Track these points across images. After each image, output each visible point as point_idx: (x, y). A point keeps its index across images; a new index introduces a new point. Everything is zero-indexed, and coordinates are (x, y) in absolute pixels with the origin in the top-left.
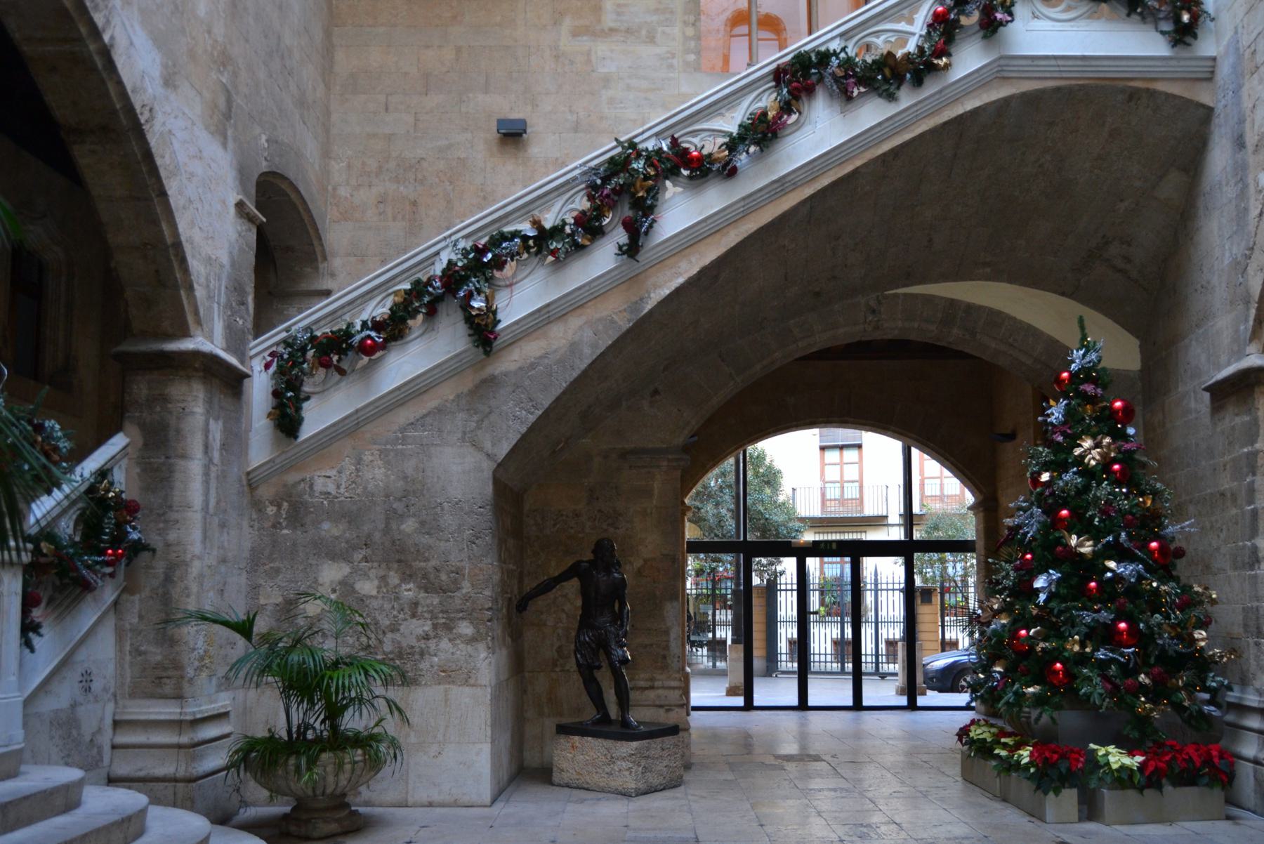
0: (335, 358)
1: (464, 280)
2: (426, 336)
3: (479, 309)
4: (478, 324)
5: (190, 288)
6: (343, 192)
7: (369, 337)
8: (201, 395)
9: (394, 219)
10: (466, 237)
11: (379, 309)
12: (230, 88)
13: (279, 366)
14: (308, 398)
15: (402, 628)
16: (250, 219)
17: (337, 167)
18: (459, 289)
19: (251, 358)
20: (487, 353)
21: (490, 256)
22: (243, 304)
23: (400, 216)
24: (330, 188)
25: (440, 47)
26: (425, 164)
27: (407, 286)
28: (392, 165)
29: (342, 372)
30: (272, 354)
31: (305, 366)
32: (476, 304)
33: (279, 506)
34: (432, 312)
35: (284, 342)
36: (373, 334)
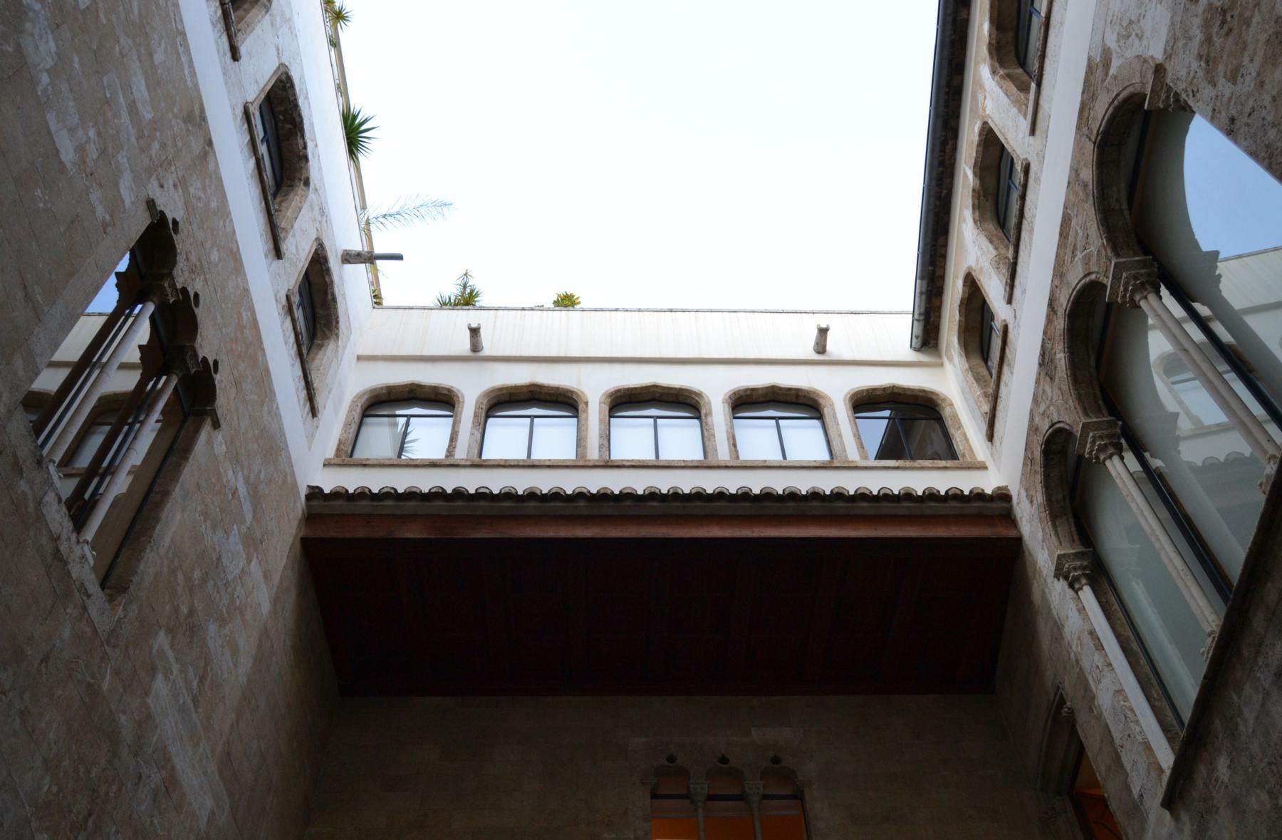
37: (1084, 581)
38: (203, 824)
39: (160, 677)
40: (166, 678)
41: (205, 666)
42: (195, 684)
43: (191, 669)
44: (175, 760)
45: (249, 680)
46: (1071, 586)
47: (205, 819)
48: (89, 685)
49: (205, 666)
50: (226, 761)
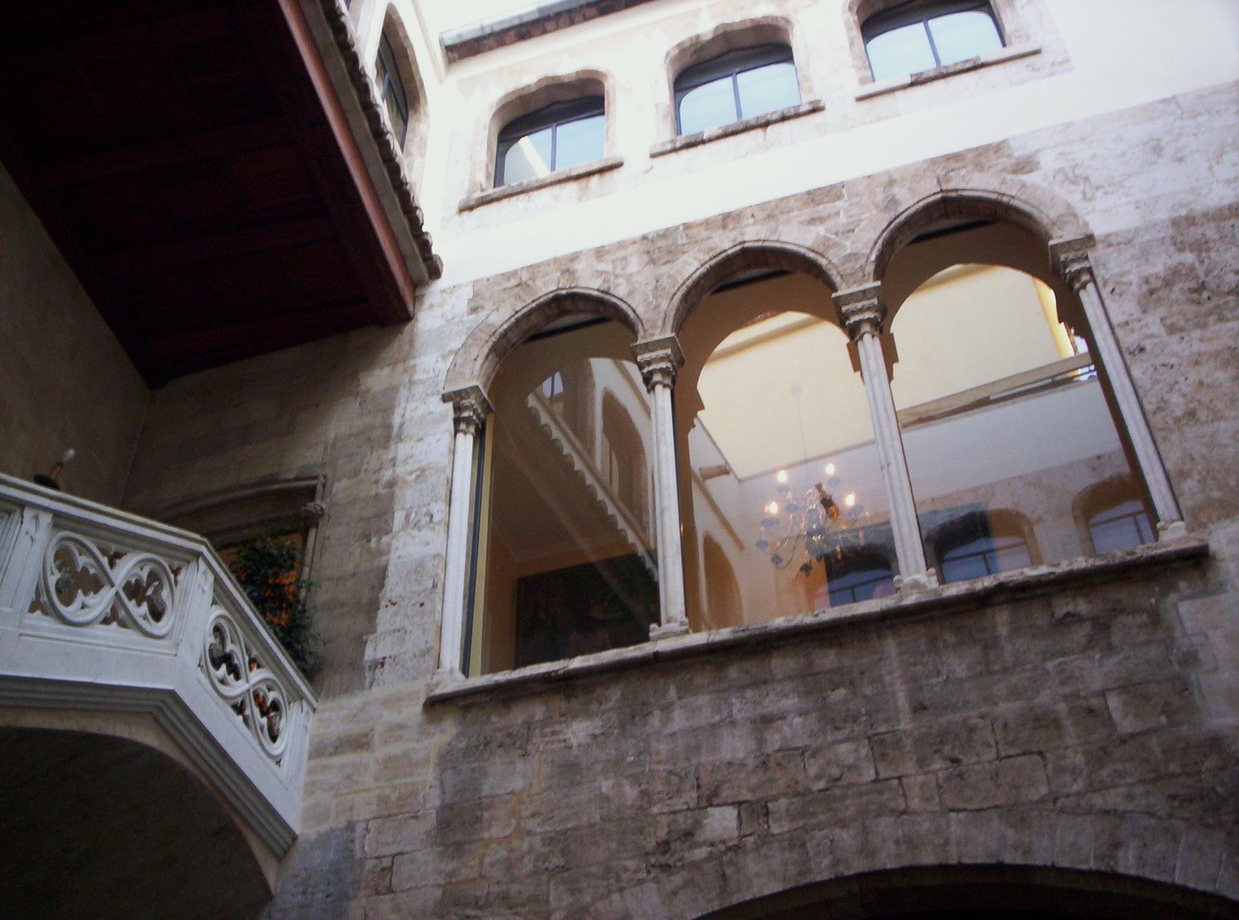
37: (472, 429)
46: (457, 421)
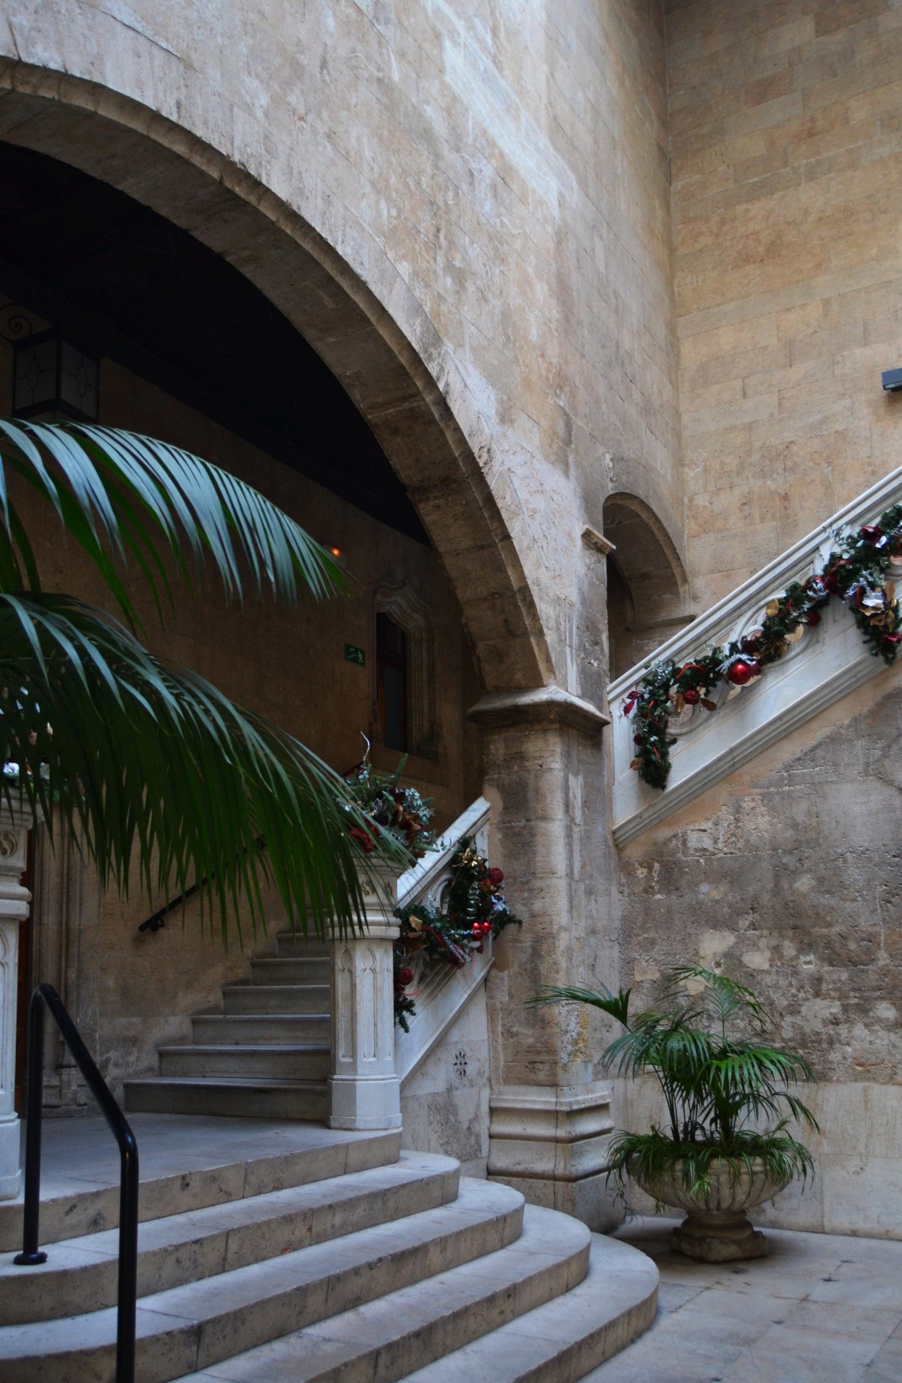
0: (702, 691)
1: (854, 575)
2: (810, 651)
3: (874, 608)
4: (876, 627)
5: (541, 634)
6: (701, 501)
7: (740, 661)
8: (558, 749)
9: (763, 520)
10: (851, 522)
11: (750, 627)
12: (568, 410)
13: (640, 708)
14: (674, 741)
15: (803, 1010)
16: (598, 548)
17: (692, 474)
18: (847, 587)
19: (609, 703)
20: (890, 661)
21: (884, 539)
22: (597, 643)
23: (769, 515)
24: (686, 500)
25: (803, 306)
26: (795, 449)
27: (782, 594)
28: (756, 457)
29: (711, 707)
30: (632, 696)
31: (669, 704)
32: (869, 602)
33: (650, 868)
34: (814, 620)
35: (645, 680)
36: (744, 657)
38: (556, 212)
39: (448, 44)
40: (456, 44)
41: (492, 13)
42: (489, 40)
43: (478, 23)
44: (501, 143)
45: (549, 15)
47: (555, 204)
48: (380, 81)
49: (492, 13)
50: (556, 128)
